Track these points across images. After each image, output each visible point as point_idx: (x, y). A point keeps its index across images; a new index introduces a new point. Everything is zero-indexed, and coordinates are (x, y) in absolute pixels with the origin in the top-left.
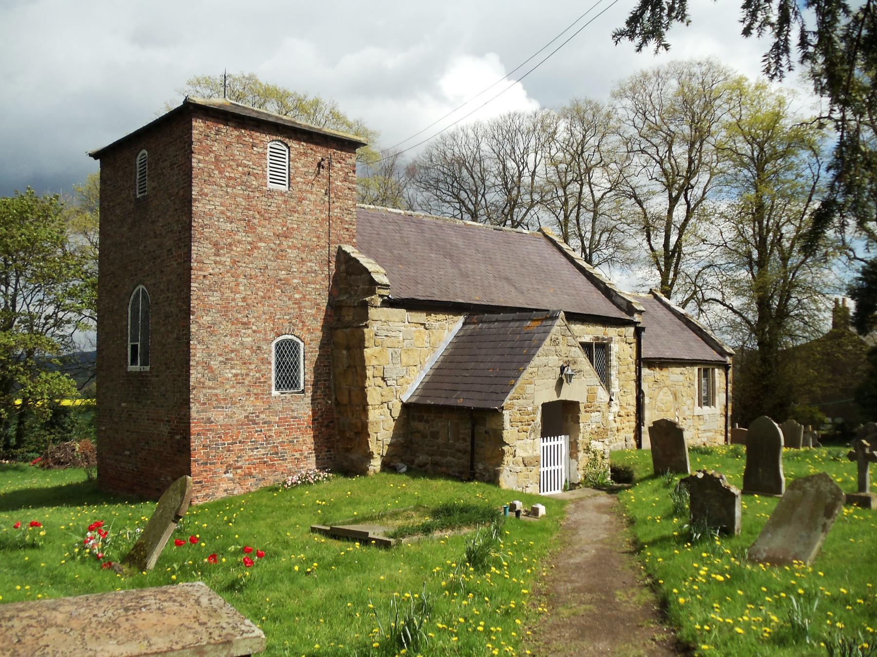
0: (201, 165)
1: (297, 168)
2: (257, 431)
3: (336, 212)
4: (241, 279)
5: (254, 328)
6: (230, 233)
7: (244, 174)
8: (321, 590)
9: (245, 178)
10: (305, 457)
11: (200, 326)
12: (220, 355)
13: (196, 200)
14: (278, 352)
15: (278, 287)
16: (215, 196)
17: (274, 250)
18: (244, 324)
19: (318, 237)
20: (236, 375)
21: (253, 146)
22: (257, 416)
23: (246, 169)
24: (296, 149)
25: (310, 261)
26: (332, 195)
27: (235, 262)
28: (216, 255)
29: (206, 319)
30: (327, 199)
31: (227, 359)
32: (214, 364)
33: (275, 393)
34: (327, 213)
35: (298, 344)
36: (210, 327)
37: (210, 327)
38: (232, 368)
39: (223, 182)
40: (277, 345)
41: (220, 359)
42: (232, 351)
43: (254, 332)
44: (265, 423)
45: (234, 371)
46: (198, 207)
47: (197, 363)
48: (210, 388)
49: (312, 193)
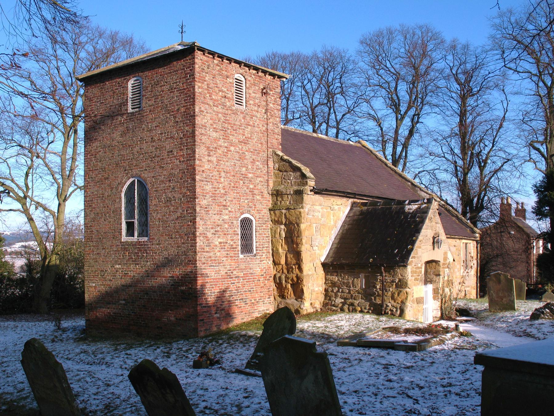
0: (200, 90)
1: (250, 94)
2: (232, 283)
3: (270, 126)
4: (223, 174)
5: (229, 209)
6: (216, 140)
7: (223, 97)
8: (442, 404)
9: (223, 100)
10: (257, 302)
11: (201, 207)
12: (212, 228)
13: (197, 116)
14: (241, 226)
15: (241, 180)
16: (207, 113)
17: (238, 153)
18: (224, 206)
19: (261, 144)
20: (220, 243)
21: (227, 77)
22: (232, 273)
23: (223, 93)
24: (249, 81)
25: (258, 161)
26: (268, 114)
27: (218, 161)
28: (209, 156)
29: (204, 202)
30: (266, 117)
31: (216, 231)
32: (209, 235)
33: (241, 256)
34: (266, 126)
35: (252, 221)
36: (206, 208)
37: (206, 208)
38: (219, 237)
39: (211, 103)
40: (241, 221)
41: (212, 231)
42: (218, 226)
43: (230, 212)
44: (236, 277)
45: (219, 240)
46: (199, 120)
47: (200, 234)
48: (207, 252)
49: (258, 112)
